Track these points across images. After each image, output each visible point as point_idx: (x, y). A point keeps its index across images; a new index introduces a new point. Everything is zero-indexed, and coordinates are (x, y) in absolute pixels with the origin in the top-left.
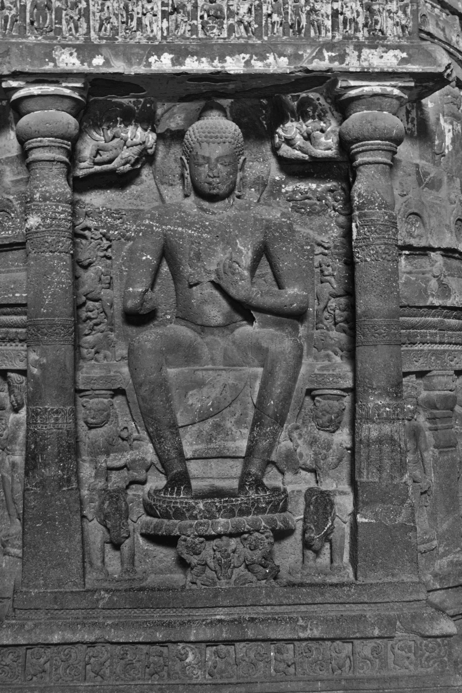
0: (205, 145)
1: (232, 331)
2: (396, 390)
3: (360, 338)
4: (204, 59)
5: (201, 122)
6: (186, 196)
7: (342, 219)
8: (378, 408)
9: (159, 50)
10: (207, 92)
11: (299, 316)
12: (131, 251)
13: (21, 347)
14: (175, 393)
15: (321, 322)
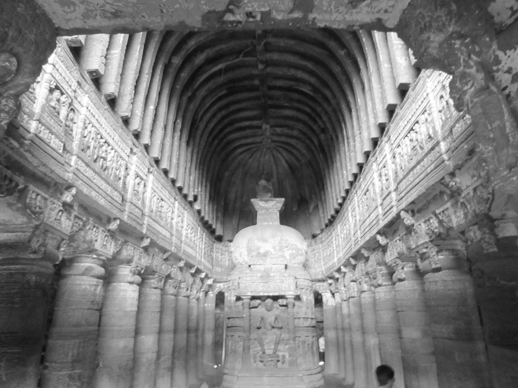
2: (294, 339)
9: (261, 292)
11: (282, 328)
13: (242, 333)
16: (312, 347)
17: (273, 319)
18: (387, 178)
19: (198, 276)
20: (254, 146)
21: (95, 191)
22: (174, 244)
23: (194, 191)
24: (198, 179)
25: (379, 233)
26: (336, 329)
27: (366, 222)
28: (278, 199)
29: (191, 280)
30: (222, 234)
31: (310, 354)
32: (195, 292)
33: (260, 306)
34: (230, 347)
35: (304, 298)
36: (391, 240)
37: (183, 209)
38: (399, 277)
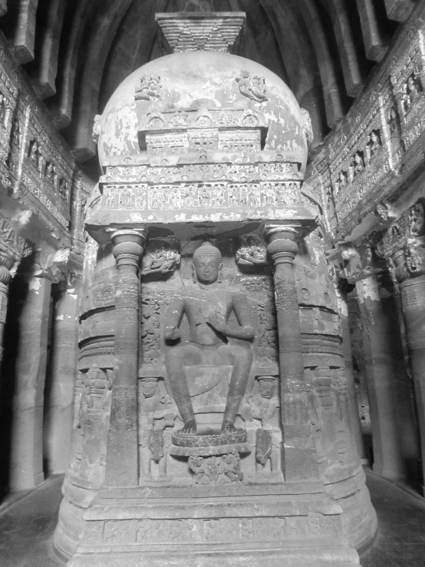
0: (202, 257)
1: (217, 347)
3: (281, 349)
4: (200, 216)
5: (201, 248)
6: (195, 283)
7: (270, 293)
8: (293, 384)
10: (203, 233)
11: (250, 340)
12: (169, 310)
14: (188, 379)
15: (262, 343)
17: (223, 307)
33: (176, 273)
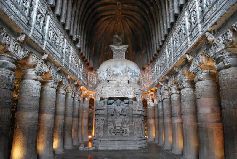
2: (132, 121)
9: (114, 95)
11: (125, 115)
16: (142, 126)
17: (121, 110)
18: (195, 17)
19: (79, 87)
20: (112, 16)
21: (7, 8)
22: (64, 63)
23: (76, 35)
24: (79, 30)
25: (187, 53)
26: (154, 118)
27: (178, 50)
28: (124, 45)
29: (75, 89)
30: (92, 66)
31: (141, 129)
32: (77, 96)
33: (113, 103)
34: (96, 125)
35: (138, 99)
36: (194, 57)
37: (69, 45)
38: (199, 78)
